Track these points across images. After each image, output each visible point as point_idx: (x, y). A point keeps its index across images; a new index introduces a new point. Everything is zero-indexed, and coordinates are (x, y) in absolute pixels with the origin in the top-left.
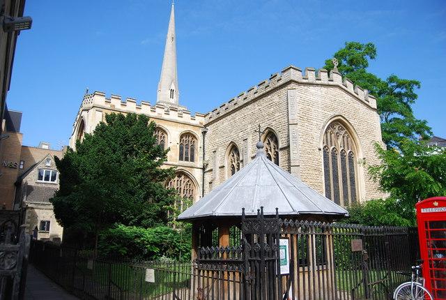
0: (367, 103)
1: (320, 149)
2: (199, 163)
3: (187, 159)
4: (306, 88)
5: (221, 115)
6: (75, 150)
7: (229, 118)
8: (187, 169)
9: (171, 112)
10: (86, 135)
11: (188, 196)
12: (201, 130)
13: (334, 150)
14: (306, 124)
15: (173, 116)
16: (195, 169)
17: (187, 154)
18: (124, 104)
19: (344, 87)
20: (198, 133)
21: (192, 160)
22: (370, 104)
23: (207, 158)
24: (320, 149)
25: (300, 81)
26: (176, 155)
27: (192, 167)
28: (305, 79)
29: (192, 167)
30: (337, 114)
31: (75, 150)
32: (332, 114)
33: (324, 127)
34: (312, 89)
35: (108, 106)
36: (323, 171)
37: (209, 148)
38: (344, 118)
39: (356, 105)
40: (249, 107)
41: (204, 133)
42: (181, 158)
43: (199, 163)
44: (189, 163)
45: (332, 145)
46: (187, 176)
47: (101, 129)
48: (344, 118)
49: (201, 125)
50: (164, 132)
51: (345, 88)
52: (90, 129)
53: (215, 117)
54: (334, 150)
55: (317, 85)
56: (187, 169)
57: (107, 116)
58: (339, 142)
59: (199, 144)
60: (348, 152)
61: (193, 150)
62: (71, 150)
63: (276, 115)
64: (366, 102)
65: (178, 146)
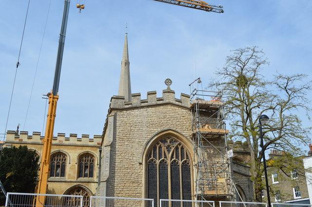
1: (140, 164)
3: (86, 176)
4: (128, 112)
8: (84, 184)
9: (71, 138)
12: (98, 150)
14: (126, 143)
16: (93, 184)
19: (177, 103)
20: (96, 153)
21: (91, 175)
25: (122, 107)
26: (74, 173)
27: (89, 182)
30: (166, 128)
33: (147, 144)
34: (136, 112)
35: (17, 140)
36: (143, 180)
38: (177, 132)
41: (100, 151)
42: (79, 175)
43: (95, 179)
44: (86, 179)
46: (84, 190)
48: (174, 131)
50: (64, 155)
51: (180, 104)
54: (163, 163)
55: (143, 107)
56: (84, 184)
59: (96, 162)
60: (180, 163)
61: (92, 168)
65: (77, 165)
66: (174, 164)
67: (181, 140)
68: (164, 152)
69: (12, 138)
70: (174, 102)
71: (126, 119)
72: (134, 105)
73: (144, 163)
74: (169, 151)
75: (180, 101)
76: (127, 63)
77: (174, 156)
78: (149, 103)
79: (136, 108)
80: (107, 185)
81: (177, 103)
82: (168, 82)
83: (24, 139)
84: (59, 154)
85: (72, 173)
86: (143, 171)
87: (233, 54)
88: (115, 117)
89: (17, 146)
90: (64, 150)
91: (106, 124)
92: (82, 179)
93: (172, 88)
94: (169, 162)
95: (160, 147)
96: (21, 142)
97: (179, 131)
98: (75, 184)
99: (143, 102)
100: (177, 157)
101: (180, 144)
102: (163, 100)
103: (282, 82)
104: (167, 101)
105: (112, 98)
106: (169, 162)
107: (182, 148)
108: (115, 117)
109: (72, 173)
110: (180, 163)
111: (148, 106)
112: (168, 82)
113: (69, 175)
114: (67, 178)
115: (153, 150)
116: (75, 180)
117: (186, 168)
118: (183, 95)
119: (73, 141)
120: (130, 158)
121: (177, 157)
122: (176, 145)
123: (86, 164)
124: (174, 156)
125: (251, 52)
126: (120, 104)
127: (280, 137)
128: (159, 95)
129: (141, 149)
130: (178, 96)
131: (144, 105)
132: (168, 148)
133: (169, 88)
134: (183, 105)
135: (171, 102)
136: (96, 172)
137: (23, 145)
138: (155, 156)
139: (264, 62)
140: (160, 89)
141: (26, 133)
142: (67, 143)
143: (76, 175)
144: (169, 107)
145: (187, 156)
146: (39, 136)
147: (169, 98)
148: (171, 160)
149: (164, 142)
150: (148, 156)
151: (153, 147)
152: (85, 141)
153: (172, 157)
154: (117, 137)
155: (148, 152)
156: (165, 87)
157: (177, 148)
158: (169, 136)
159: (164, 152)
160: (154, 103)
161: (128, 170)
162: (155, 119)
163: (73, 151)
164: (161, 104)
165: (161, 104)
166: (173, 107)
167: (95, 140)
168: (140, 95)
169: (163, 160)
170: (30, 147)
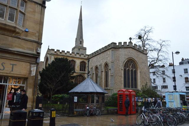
0: (143, 52)
1: (122, 70)
2: (87, 72)
3: (82, 71)
5: (94, 55)
6: (45, 69)
7: (96, 57)
10: (49, 64)
13: (128, 70)
15: (78, 56)
17: (82, 69)
19: (134, 47)
20: (87, 62)
21: (85, 71)
23: (89, 70)
24: (122, 70)
26: (79, 69)
27: (84, 73)
29: (84, 73)
30: (130, 57)
31: (45, 69)
34: (120, 50)
35: (56, 54)
36: (123, 77)
37: (90, 67)
40: (102, 54)
41: (89, 61)
42: (80, 70)
45: (128, 68)
46: (82, 76)
47: (53, 62)
52: (50, 62)
53: (92, 56)
57: (55, 59)
58: (131, 67)
59: (87, 65)
62: (44, 69)
63: (109, 58)
64: (143, 52)
66: (132, 70)
67: (134, 62)
73: (123, 70)
75: (134, 47)
76: (81, 20)
78: (125, 46)
79: (120, 48)
81: (134, 47)
82: (130, 39)
83: (59, 54)
84: (73, 61)
85: (78, 69)
86: (123, 72)
87: (143, 28)
89: (60, 57)
90: (75, 60)
93: (132, 41)
95: (127, 64)
96: (58, 55)
99: (123, 46)
100: (133, 68)
103: (161, 42)
107: (134, 65)
109: (78, 69)
111: (124, 48)
112: (130, 39)
115: (126, 65)
116: (79, 72)
117: (136, 72)
118: (135, 44)
119: (78, 56)
121: (133, 68)
123: (83, 66)
125: (150, 28)
127: (156, 62)
128: (128, 44)
132: (130, 65)
133: (131, 41)
136: (87, 69)
137: (65, 57)
140: (128, 41)
141: (53, 50)
150: (124, 67)
151: (126, 63)
152: (82, 56)
156: (129, 41)
157: (132, 65)
158: (131, 59)
160: (126, 47)
167: (86, 56)
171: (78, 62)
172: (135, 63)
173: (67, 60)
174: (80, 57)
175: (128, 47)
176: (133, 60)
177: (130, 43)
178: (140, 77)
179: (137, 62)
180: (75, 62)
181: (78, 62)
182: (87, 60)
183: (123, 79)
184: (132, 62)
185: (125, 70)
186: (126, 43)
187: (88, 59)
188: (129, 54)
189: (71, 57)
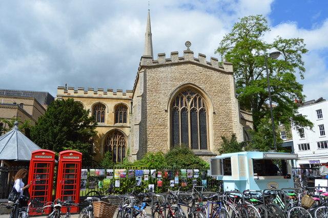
1: (166, 111)
3: (121, 122)
8: (119, 128)
11: (121, 145)
15: (110, 95)
18: (76, 92)
19: (196, 62)
21: (125, 121)
22: (225, 70)
25: (150, 65)
27: (123, 127)
28: (155, 62)
29: (123, 127)
30: (186, 82)
32: (181, 83)
34: (162, 69)
35: (66, 94)
38: (197, 86)
39: (208, 73)
41: (132, 103)
42: (116, 121)
44: (121, 124)
49: (130, 98)
51: (198, 62)
54: (184, 110)
56: (119, 128)
58: (190, 104)
59: (128, 111)
60: (198, 110)
66: (193, 111)
67: (199, 92)
68: (185, 102)
69: (61, 92)
70: (193, 61)
71: (153, 75)
72: (160, 63)
74: (189, 101)
76: (150, 35)
77: (193, 105)
80: (140, 128)
81: (196, 62)
82: (188, 44)
83: (72, 93)
85: (110, 121)
86: (169, 116)
88: (145, 72)
90: (104, 102)
91: (138, 79)
92: (118, 124)
93: (191, 48)
94: (189, 109)
97: (197, 85)
98: (113, 128)
100: (195, 106)
101: (198, 95)
102: (184, 59)
104: (187, 60)
105: (142, 57)
106: (189, 109)
108: (145, 72)
110: (198, 110)
113: (108, 121)
114: (106, 124)
115: (176, 100)
116: (112, 125)
117: (203, 112)
118: (200, 55)
119: (110, 95)
120: (159, 106)
121: (195, 106)
122: (194, 96)
123: (121, 111)
124: (193, 105)
126: (148, 62)
128: (181, 55)
129: (167, 99)
130: (196, 56)
131: (169, 64)
132: (189, 99)
133: (188, 49)
134: (201, 63)
135: (191, 60)
138: (178, 105)
139: (265, 29)
142: (105, 96)
143: (113, 121)
144: (189, 65)
145: (203, 105)
146: (83, 91)
147: (188, 58)
148: (191, 108)
149: (185, 93)
150: (173, 104)
152: (119, 95)
153: (191, 106)
154: (147, 89)
155: (172, 102)
156: (186, 49)
157: (195, 99)
159: (185, 102)
160: (176, 61)
161: (156, 116)
162: (177, 75)
163: (110, 103)
164: (182, 62)
165: (182, 62)
166: (192, 65)
168: (164, 55)
169: (184, 108)
170: (76, 100)
171: (110, 107)
172: (202, 94)
173: (73, 102)
174: (115, 97)
175: (182, 61)
176: (197, 90)
177: (188, 52)
178: (215, 123)
179: (207, 94)
180: (99, 108)
181: (110, 107)
182: (130, 101)
183: (168, 131)
184: (192, 94)
185: (173, 112)
186: (176, 53)
187: (129, 100)
188: (185, 76)
189: (95, 98)
